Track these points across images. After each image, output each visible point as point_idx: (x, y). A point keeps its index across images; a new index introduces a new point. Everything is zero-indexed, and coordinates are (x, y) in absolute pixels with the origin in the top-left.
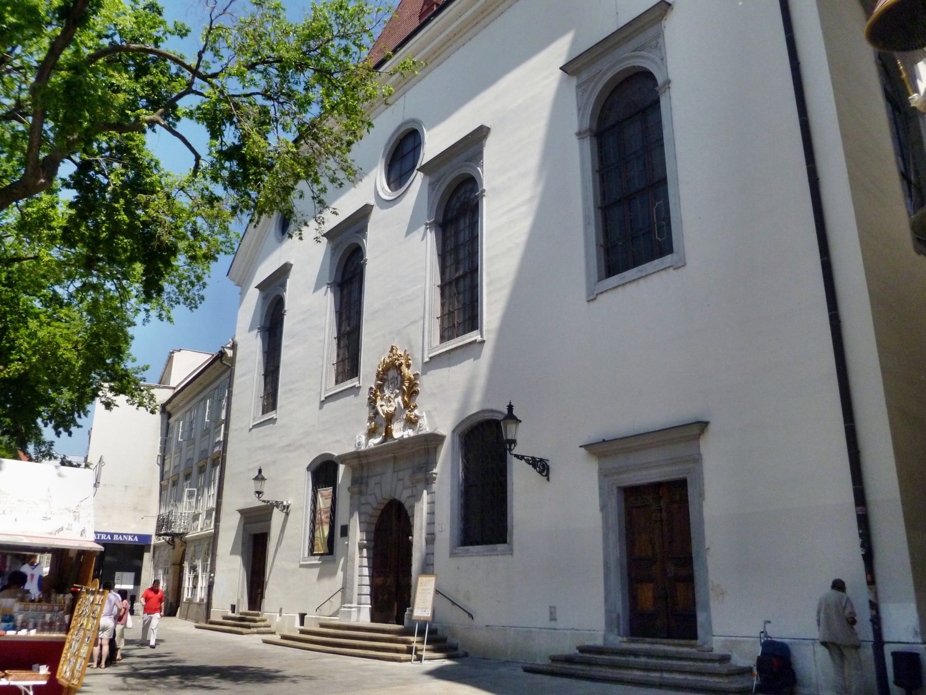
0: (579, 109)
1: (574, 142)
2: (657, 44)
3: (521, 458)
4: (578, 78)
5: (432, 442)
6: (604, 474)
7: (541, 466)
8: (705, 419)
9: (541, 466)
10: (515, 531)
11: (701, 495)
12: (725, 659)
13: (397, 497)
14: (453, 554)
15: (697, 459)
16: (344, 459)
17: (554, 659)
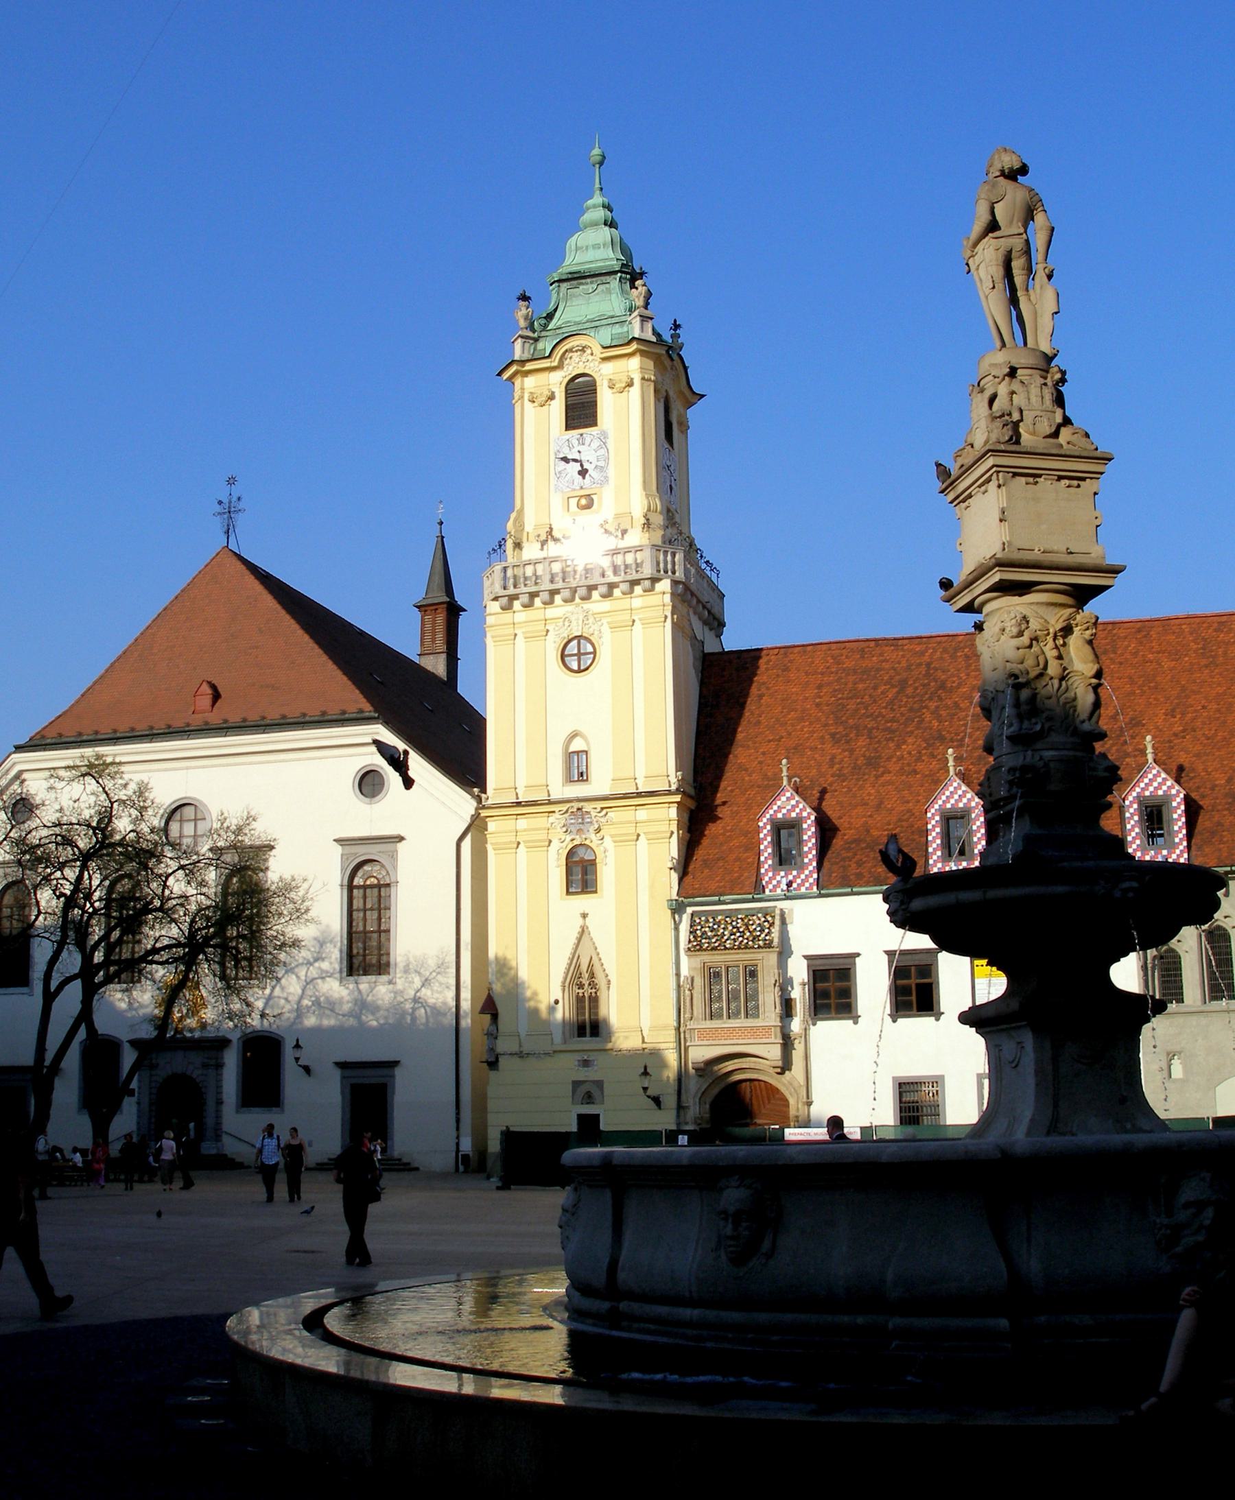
0: (342, 870)
1: (338, 889)
2: (393, 856)
3: (300, 1066)
4: (343, 850)
5: (222, 1043)
6: (343, 1078)
7: (307, 1069)
8: (397, 1059)
9: (307, 1069)
10: (286, 1101)
11: (393, 1093)
12: (400, 1160)
13: (188, 1073)
14: (237, 1112)
15: (393, 1076)
16: (134, 1043)
17: (318, 1164)
